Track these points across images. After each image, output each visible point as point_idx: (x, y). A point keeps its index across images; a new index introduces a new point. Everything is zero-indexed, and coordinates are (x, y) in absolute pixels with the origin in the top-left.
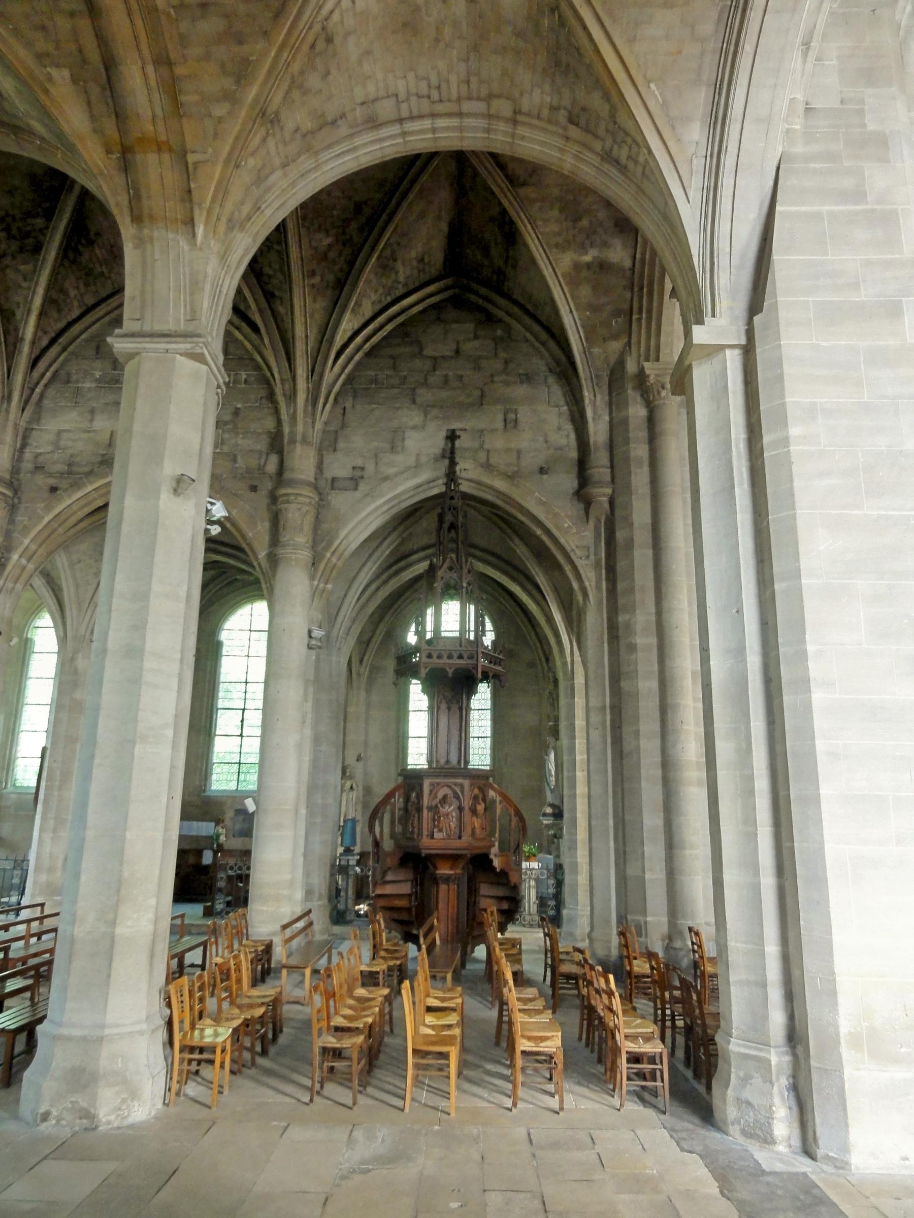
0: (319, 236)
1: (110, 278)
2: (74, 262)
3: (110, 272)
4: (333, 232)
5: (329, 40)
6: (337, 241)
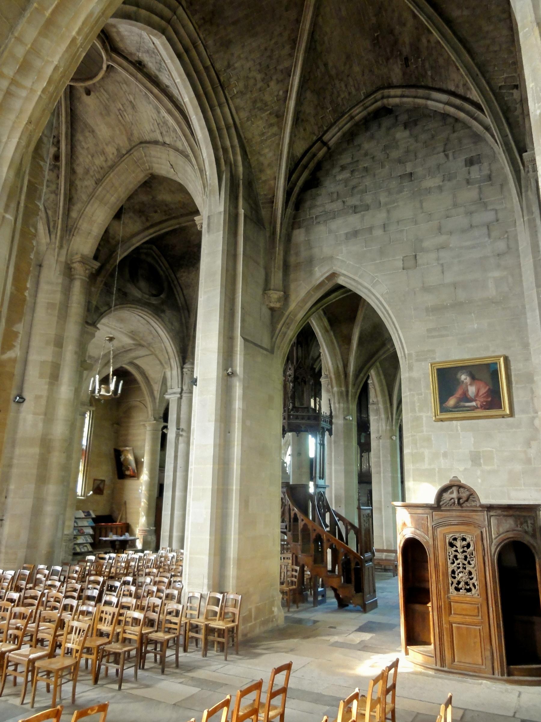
5: (132, 331)
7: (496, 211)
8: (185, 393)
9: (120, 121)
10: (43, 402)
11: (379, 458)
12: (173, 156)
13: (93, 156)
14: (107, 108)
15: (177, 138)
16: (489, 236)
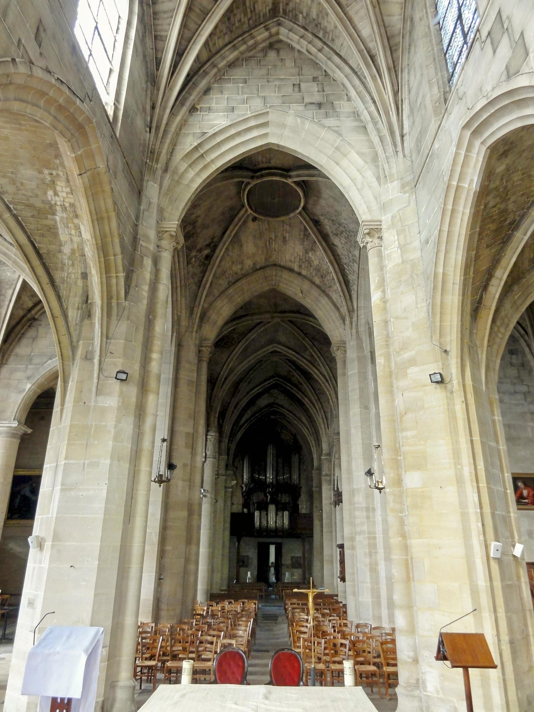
7: (528, 386)
8: (209, 458)
9: (266, 245)
10: (188, 469)
12: (306, 285)
13: (233, 263)
14: (261, 235)
15: (316, 275)
16: (526, 401)
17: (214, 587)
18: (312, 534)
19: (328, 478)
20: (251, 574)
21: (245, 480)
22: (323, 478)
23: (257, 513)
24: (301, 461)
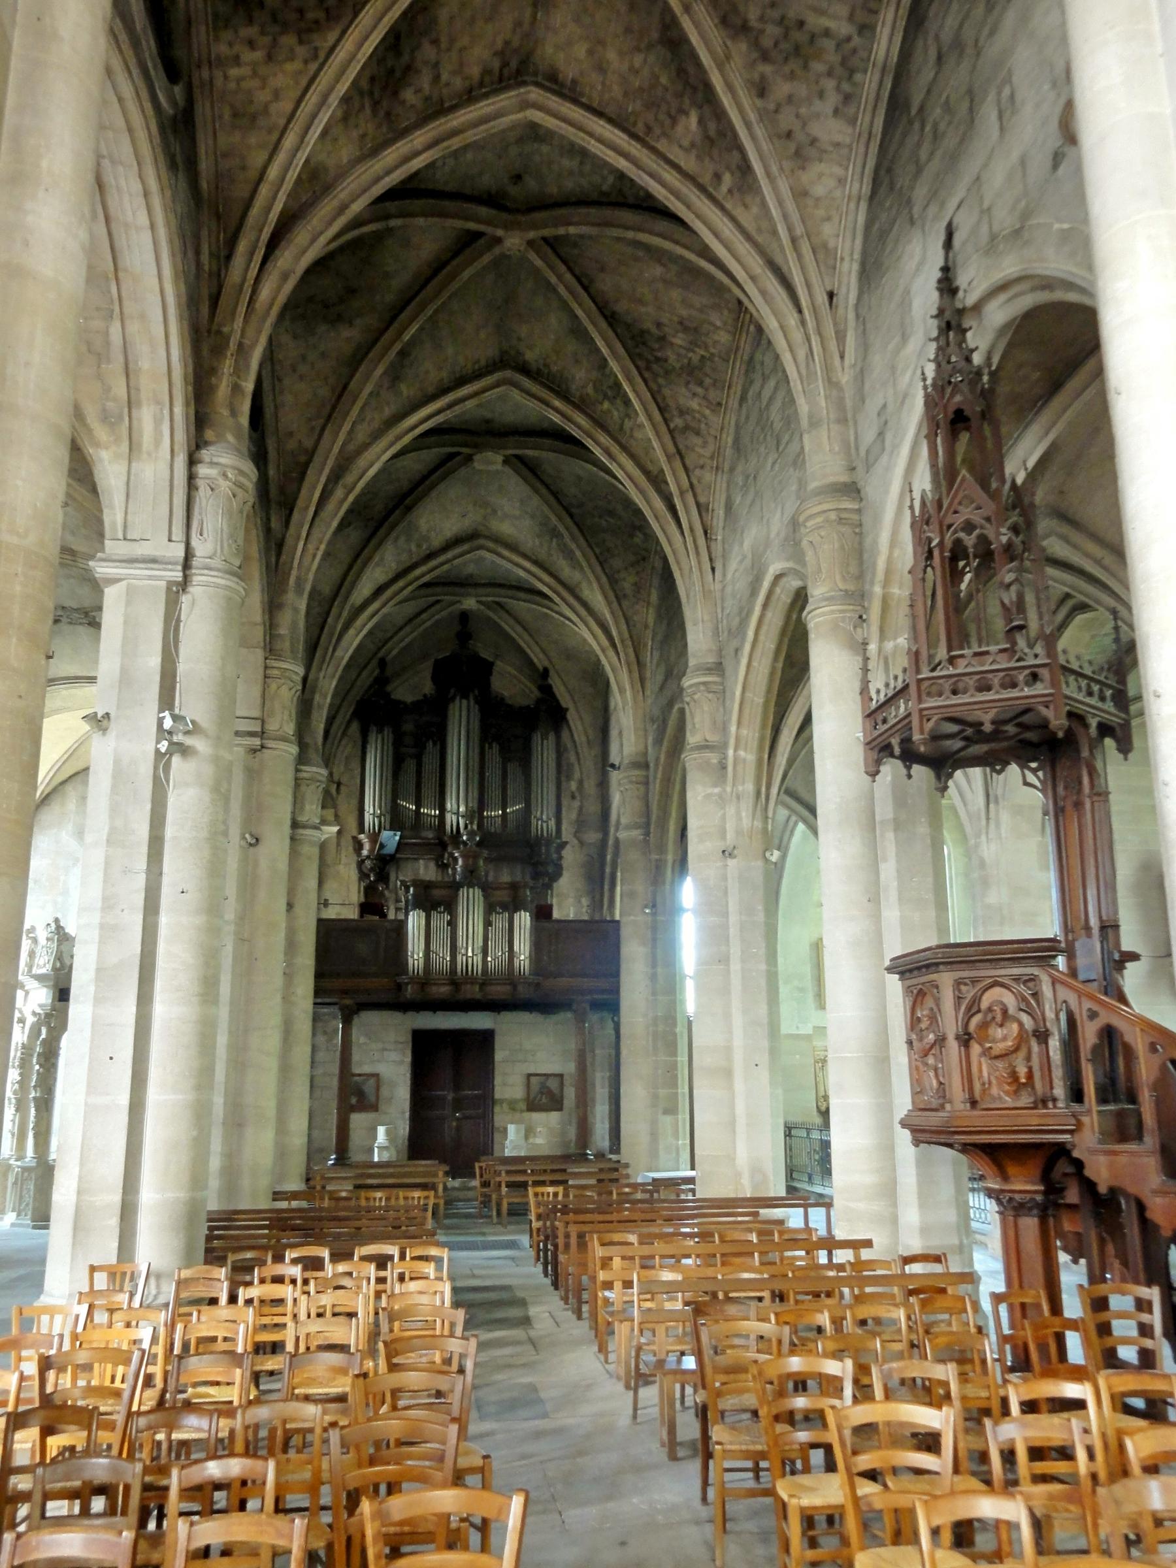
0: (680, 129)
1: (712, 355)
2: (667, 373)
3: (706, 348)
4: (687, 101)
6: (701, 107)
11: (726, 914)
17: (246, 1182)
18: (616, 990)
19: (714, 758)
20: (388, 1133)
21: (368, 818)
22: (690, 759)
23: (415, 922)
24: (562, 771)
